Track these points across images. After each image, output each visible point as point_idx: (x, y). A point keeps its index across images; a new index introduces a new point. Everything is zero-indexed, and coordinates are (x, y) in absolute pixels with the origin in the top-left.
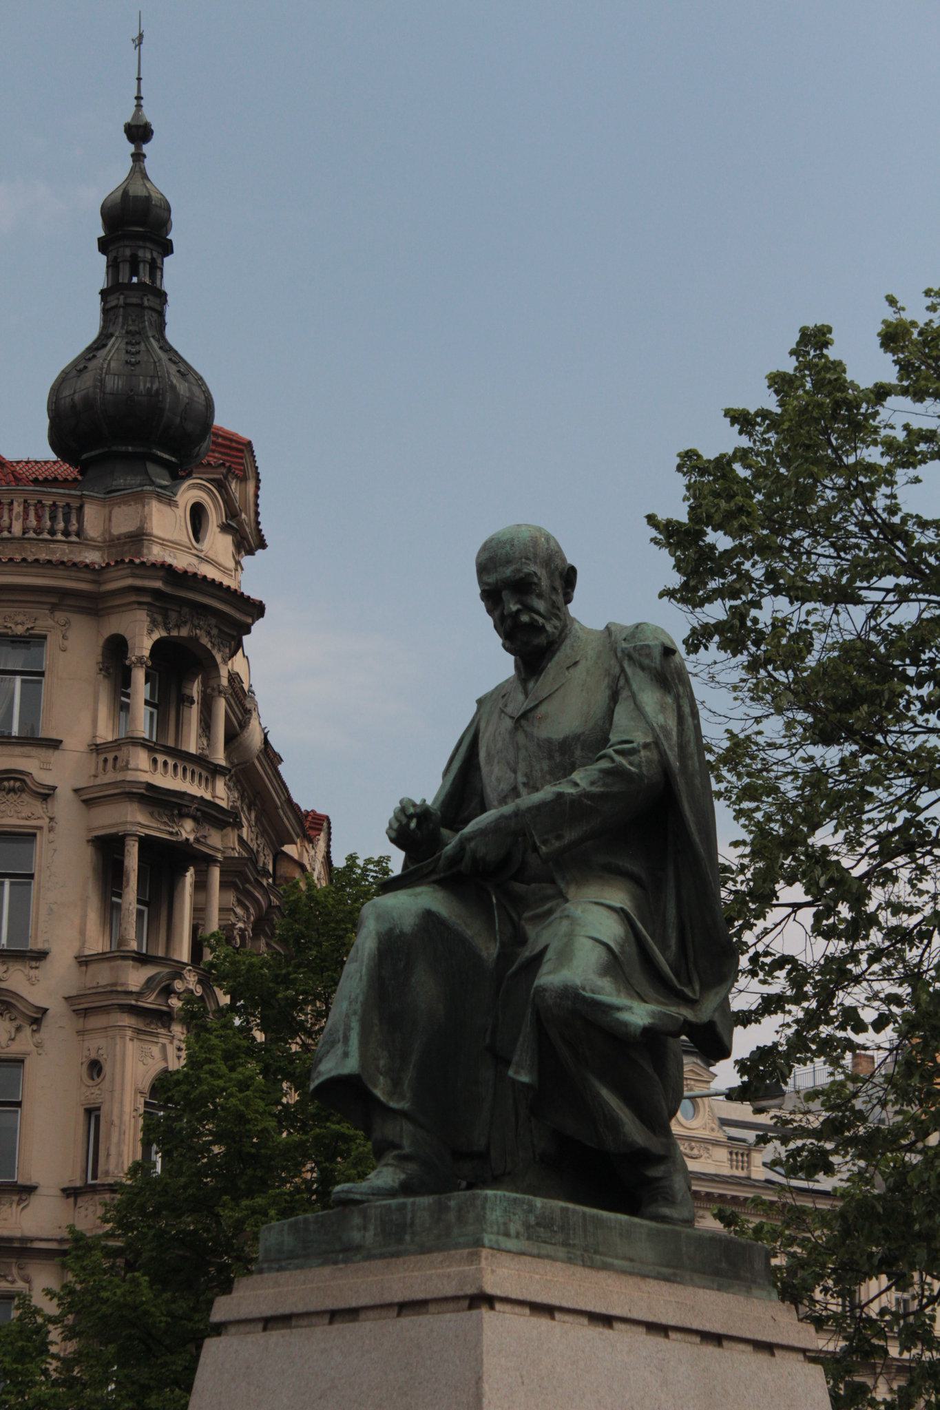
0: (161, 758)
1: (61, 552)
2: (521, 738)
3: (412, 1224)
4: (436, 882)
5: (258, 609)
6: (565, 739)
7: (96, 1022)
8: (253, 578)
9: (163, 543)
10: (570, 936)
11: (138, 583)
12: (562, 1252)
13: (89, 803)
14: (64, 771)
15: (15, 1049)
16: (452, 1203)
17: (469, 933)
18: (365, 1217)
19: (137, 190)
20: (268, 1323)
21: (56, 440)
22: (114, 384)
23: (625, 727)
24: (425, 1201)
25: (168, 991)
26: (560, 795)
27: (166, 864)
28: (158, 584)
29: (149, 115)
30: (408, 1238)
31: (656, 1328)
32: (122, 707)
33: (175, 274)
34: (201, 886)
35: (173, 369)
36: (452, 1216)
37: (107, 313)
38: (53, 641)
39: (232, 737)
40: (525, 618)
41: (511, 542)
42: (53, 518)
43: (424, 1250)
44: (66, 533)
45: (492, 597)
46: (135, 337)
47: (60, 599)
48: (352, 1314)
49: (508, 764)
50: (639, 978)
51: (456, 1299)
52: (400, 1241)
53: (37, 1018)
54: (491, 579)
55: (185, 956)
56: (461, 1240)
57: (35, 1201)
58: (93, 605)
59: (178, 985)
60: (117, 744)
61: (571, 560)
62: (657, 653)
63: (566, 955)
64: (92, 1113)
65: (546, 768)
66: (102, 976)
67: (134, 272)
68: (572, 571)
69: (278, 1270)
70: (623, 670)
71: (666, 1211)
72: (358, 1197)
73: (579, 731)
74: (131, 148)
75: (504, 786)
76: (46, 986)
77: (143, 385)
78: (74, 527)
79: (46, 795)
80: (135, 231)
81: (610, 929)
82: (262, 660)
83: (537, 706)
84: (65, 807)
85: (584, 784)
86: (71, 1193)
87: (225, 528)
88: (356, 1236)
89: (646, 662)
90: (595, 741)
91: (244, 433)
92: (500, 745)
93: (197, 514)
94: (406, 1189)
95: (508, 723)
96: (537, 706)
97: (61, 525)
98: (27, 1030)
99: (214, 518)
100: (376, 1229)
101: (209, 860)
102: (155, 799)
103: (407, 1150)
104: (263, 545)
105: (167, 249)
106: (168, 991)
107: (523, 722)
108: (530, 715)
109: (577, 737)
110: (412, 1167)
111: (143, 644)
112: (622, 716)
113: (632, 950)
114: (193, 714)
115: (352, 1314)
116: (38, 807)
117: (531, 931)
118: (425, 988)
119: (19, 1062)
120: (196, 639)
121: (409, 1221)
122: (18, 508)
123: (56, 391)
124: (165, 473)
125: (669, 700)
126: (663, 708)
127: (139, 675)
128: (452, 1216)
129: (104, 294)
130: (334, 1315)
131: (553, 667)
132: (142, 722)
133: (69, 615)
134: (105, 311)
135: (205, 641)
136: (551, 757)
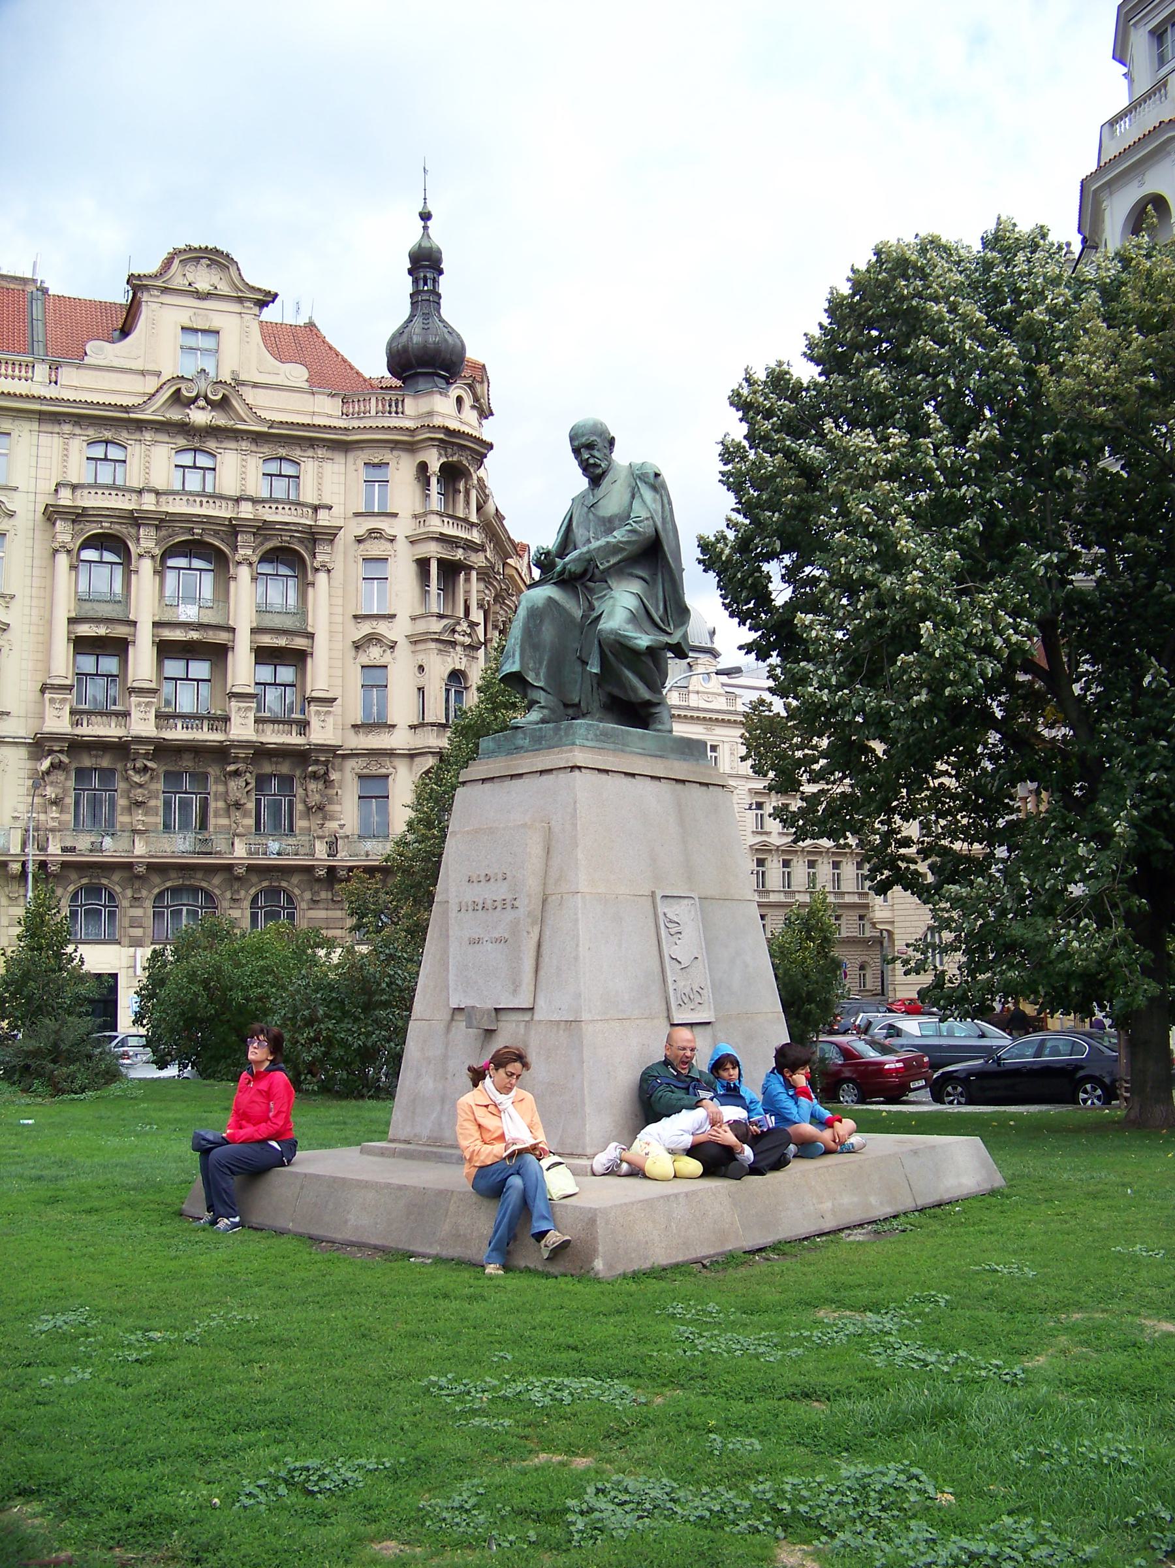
0: (446, 520)
5: (490, 446)
7: (420, 647)
8: (487, 431)
9: (443, 416)
10: (614, 606)
11: (432, 436)
12: (612, 746)
14: (401, 528)
17: (568, 606)
18: (525, 734)
19: (425, 244)
23: (638, 510)
24: (551, 725)
25: (454, 631)
26: (608, 543)
27: (450, 571)
28: (441, 436)
29: (431, 207)
33: (445, 285)
34: (468, 580)
35: (445, 330)
39: (479, 508)
40: (591, 461)
41: (584, 426)
42: (390, 406)
44: (397, 413)
45: (576, 451)
46: (426, 316)
47: (395, 445)
48: (520, 775)
50: (647, 625)
54: (576, 443)
55: (462, 616)
57: (396, 731)
58: (410, 447)
59: (458, 628)
60: (425, 514)
61: (612, 434)
62: (652, 475)
63: (611, 614)
64: (421, 690)
66: (421, 626)
67: (425, 284)
68: (613, 438)
71: (659, 727)
74: (422, 223)
75: (584, 539)
76: (396, 631)
77: (431, 339)
78: (400, 410)
80: (425, 264)
81: (632, 603)
82: (492, 471)
84: (402, 545)
85: (619, 538)
87: (473, 407)
88: (520, 742)
90: (625, 517)
91: (482, 361)
93: (459, 400)
94: (543, 721)
95: (586, 509)
97: (394, 409)
98: (389, 651)
99: (468, 401)
101: (471, 568)
102: (443, 539)
104: (492, 414)
105: (441, 272)
106: (454, 631)
110: (546, 711)
111: (434, 466)
112: (636, 504)
113: (642, 611)
116: (388, 545)
117: (596, 604)
118: (548, 633)
120: (460, 462)
122: (373, 401)
123: (390, 344)
124: (443, 381)
125: (658, 497)
126: (655, 501)
127: (434, 480)
129: (412, 296)
130: (512, 776)
131: (605, 483)
132: (436, 502)
133: (401, 453)
134: (412, 304)
135: (465, 462)
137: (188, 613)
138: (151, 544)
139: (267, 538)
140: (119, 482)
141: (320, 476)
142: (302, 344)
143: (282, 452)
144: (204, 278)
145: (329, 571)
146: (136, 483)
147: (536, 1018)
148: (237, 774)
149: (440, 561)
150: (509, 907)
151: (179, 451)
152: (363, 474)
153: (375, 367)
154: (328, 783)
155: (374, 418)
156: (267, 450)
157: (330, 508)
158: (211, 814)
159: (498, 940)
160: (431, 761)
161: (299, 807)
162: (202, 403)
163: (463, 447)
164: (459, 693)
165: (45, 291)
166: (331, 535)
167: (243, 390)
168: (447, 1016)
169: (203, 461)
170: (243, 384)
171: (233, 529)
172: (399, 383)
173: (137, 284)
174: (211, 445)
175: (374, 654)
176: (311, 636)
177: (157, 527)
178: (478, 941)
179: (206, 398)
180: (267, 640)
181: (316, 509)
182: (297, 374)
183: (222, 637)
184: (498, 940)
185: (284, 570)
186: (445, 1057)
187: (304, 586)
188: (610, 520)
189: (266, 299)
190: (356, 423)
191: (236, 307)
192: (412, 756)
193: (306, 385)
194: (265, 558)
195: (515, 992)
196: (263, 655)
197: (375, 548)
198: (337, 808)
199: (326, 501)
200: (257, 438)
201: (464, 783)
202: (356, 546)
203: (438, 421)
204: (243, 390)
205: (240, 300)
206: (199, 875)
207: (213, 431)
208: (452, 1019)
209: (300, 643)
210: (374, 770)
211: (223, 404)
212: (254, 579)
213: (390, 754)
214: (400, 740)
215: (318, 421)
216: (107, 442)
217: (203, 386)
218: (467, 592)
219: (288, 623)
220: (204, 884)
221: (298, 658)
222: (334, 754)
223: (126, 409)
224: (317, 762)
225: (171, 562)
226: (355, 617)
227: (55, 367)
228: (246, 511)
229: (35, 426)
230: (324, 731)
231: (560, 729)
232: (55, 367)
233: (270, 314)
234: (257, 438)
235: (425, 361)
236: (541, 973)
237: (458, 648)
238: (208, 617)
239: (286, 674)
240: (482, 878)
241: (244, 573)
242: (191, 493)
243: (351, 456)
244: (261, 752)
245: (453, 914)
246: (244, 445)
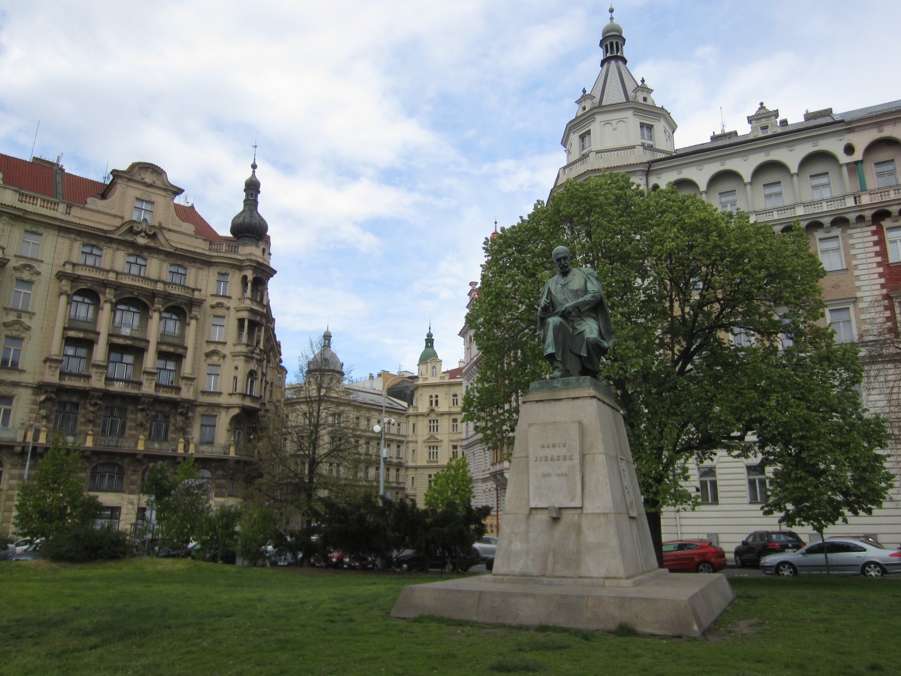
1: (233, 256)
5: (275, 272)
7: (236, 358)
8: (273, 265)
13: (237, 311)
15: (219, 363)
20: (537, 401)
21: (233, 230)
22: (247, 220)
31: (608, 405)
32: (245, 291)
33: (260, 198)
34: (260, 331)
37: (245, 205)
38: (231, 274)
43: (574, 387)
47: (233, 266)
48: (560, 400)
53: (224, 357)
63: (591, 332)
64: (235, 378)
77: (253, 221)
79: (228, 308)
82: (273, 285)
84: (232, 312)
86: (230, 395)
102: (251, 311)
105: (259, 192)
106: (253, 352)
114: (259, 293)
115: (560, 400)
116: (226, 311)
117: (578, 327)
119: (219, 366)
127: (249, 285)
129: (245, 201)
130: (555, 400)
131: (570, 275)
132: (249, 293)
137: (126, 331)
138: (112, 297)
139: (169, 301)
140: (97, 265)
141: (197, 276)
142: (189, 214)
143: (179, 262)
144: (149, 178)
145: (197, 319)
146: (107, 267)
147: (585, 511)
148: (142, 410)
149: (250, 321)
150: (567, 459)
151: (129, 255)
152: (216, 277)
153: (224, 231)
154: (187, 418)
155: (223, 252)
156: (172, 260)
157: (200, 290)
158: (127, 428)
159: (561, 475)
160: (236, 411)
161: (172, 428)
162: (143, 234)
163: (264, 271)
164: (252, 382)
165: (63, 170)
166: (200, 303)
167: (164, 231)
168: (526, 511)
169: (140, 261)
170: (164, 228)
171: (153, 294)
172: (235, 239)
173: (116, 174)
174: (146, 254)
175: (215, 359)
176: (186, 348)
177: (116, 290)
178: (549, 475)
179: (145, 232)
180: (164, 348)
181: (193, 290)
182: (189, 228)
183: (143, 344)
184: (561, 475)
185: (174, 317)
186: (527, 532)
187: (184, 324)
188: (576, 291)
189: (178, 191)
190: (215, 254)
191: (163, 193)
192: (228, 408)
193: (193, 233)
194: (166, 311)
195: (572, 500)
196: (162, 355)
197: (220, 312)
198: (190, 429)
199: (199, 287)
200: (168, 254)
202: (210, 309)
203: (253, 258)
204: (164, 231)
205: (166, 190)
206: (118, 458)
207: (146, 248)
208: (530, 513)
209: (180, 351)
210: (210, 412)
211: (153, 237)
212: (161, 318)
213: (219, 406)
214: (223, 400)
215: (197, 250)
216: (93, 246)
217: (144, 226)
218: (259, 336)
219: (176, 341)
220: (120, 462)
221: (178, 358)
222: (192, 405)
223: (105, 231)
224: (183, 407)
225: (119, 307)
226: (208, 342)
227: (69, 206)
228: (160, 287)
229: (56, 233)
230: (187, 393)
232: (69, 206)
233: (179, 200)
234: (168, 254)
235: (251, 229)
236: (586, 491)
237: (254, 361)
238: (136, 334)
239: (171, 366)
240: (550, 445)
241: (156, 316)
242: (134, 276)
243: (212, 269)
244: (156, 400)
245: (531, 464)
246: (162, 257)
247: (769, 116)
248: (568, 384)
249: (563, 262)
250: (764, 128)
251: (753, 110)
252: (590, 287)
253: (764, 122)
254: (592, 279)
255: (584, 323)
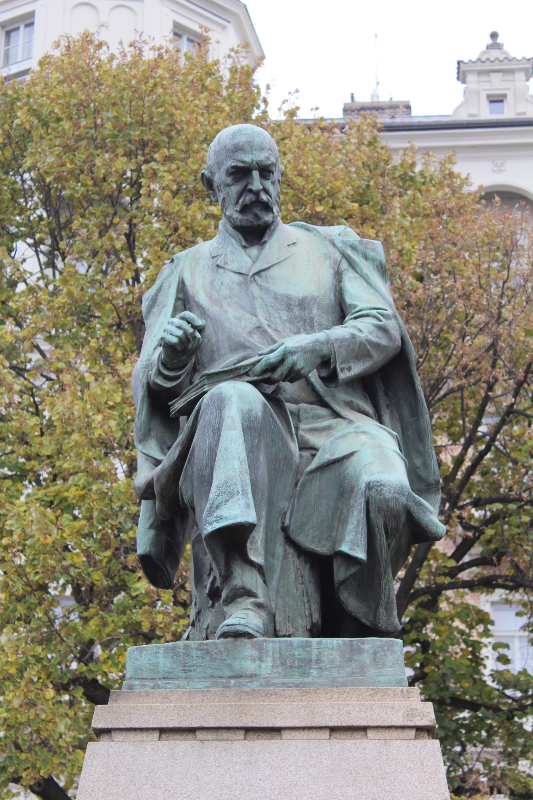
2: (254, 289)
3: (318, 661)
4: (255, 383)
6: (304, 299)
16: (366, 647)
26: (353, 336)
30: (314, 672)
36: (366, 658)
40: (264, 197)
43: (334, 683)
48: (276, 731)
49: (243, 308)
51: (403, 728)
52: (305, 674)
56: (381, 679)
65: (285, 318)
69: (153, 688)
70: (345, 256)
72: (251, 632)
73: (316, 294)
83: (269, 268)
88: (250, 666)
89: (371, 254)
92: (225, 292)
96: (269, 268)
100: (274, 660)
103: (261, 600)
107: (257, 278)
108: (263, 274)
109: (314, 299)
121: (314, 657)
128: (366, 658)
136: (289, 308)
188: (303, 304)
201: (101, 733)
231: (360, 651)
247: (511, 72)
248: (304, 665)
249: (256, 183)
250: (497, 100)
251: (473, 49)
252: (357, 293)
253: (497, 84)
254: (366, 267)
255: (341, 427)
